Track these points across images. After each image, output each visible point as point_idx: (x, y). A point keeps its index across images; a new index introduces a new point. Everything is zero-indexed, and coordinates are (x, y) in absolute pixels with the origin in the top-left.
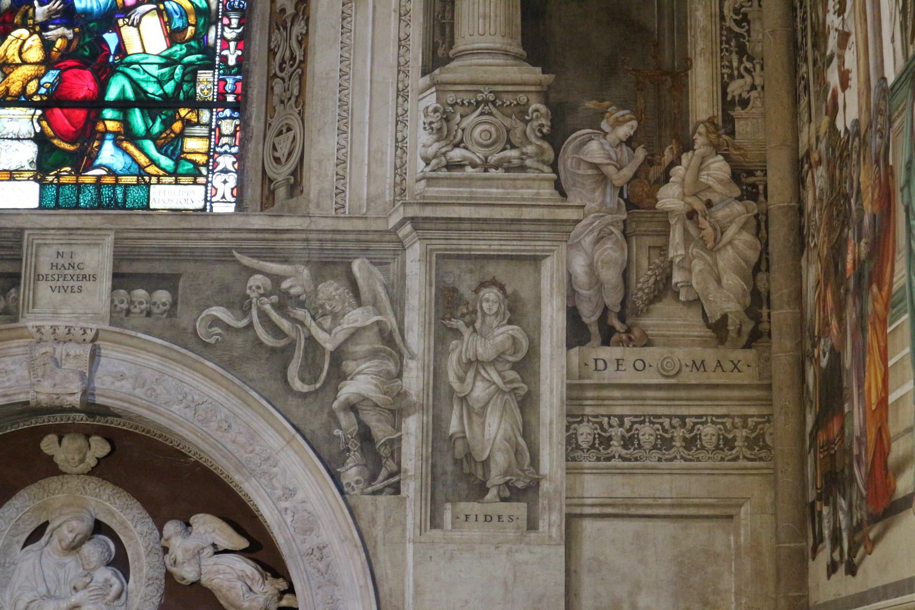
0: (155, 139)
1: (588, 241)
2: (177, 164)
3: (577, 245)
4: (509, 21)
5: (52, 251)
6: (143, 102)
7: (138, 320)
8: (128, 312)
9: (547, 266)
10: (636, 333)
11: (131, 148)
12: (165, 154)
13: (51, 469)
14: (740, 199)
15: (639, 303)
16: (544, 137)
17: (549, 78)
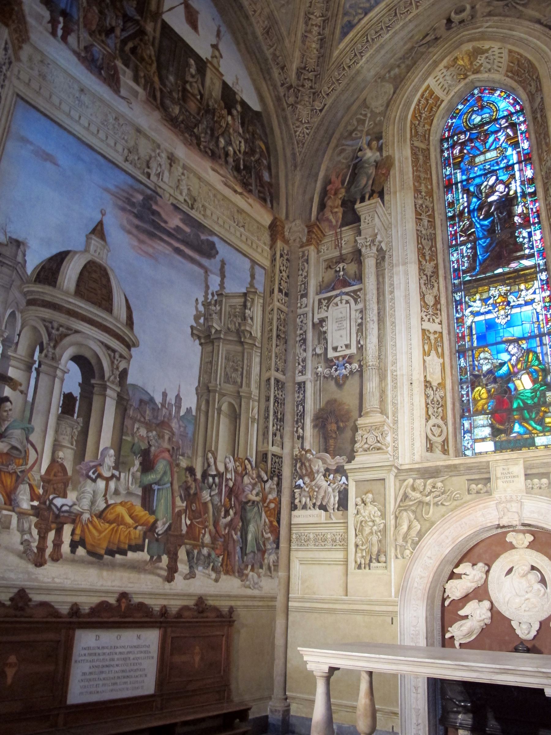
0: (534, 420)
2: (543, 428)
5: (501, 468)
6: (527, 407)
7: (536, 490)
8: (532, 488)
11: (525, 425)
12: (538, 425)
13: (512, 547)
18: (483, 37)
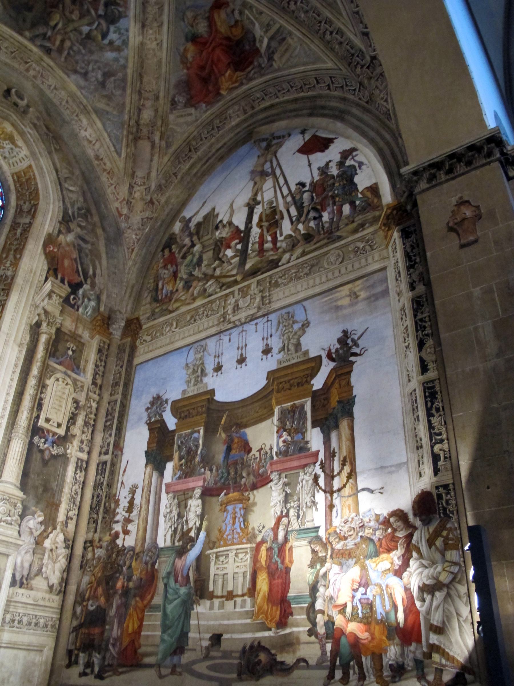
1: (23, 552)
3: (19, 553)
4: (18, 475)
9: (10, 558)
10: (29, 585)
14: (64, 548)
15: (32, 576)
16: (19, 516)
17: (25, 497)
18: (22, 134)
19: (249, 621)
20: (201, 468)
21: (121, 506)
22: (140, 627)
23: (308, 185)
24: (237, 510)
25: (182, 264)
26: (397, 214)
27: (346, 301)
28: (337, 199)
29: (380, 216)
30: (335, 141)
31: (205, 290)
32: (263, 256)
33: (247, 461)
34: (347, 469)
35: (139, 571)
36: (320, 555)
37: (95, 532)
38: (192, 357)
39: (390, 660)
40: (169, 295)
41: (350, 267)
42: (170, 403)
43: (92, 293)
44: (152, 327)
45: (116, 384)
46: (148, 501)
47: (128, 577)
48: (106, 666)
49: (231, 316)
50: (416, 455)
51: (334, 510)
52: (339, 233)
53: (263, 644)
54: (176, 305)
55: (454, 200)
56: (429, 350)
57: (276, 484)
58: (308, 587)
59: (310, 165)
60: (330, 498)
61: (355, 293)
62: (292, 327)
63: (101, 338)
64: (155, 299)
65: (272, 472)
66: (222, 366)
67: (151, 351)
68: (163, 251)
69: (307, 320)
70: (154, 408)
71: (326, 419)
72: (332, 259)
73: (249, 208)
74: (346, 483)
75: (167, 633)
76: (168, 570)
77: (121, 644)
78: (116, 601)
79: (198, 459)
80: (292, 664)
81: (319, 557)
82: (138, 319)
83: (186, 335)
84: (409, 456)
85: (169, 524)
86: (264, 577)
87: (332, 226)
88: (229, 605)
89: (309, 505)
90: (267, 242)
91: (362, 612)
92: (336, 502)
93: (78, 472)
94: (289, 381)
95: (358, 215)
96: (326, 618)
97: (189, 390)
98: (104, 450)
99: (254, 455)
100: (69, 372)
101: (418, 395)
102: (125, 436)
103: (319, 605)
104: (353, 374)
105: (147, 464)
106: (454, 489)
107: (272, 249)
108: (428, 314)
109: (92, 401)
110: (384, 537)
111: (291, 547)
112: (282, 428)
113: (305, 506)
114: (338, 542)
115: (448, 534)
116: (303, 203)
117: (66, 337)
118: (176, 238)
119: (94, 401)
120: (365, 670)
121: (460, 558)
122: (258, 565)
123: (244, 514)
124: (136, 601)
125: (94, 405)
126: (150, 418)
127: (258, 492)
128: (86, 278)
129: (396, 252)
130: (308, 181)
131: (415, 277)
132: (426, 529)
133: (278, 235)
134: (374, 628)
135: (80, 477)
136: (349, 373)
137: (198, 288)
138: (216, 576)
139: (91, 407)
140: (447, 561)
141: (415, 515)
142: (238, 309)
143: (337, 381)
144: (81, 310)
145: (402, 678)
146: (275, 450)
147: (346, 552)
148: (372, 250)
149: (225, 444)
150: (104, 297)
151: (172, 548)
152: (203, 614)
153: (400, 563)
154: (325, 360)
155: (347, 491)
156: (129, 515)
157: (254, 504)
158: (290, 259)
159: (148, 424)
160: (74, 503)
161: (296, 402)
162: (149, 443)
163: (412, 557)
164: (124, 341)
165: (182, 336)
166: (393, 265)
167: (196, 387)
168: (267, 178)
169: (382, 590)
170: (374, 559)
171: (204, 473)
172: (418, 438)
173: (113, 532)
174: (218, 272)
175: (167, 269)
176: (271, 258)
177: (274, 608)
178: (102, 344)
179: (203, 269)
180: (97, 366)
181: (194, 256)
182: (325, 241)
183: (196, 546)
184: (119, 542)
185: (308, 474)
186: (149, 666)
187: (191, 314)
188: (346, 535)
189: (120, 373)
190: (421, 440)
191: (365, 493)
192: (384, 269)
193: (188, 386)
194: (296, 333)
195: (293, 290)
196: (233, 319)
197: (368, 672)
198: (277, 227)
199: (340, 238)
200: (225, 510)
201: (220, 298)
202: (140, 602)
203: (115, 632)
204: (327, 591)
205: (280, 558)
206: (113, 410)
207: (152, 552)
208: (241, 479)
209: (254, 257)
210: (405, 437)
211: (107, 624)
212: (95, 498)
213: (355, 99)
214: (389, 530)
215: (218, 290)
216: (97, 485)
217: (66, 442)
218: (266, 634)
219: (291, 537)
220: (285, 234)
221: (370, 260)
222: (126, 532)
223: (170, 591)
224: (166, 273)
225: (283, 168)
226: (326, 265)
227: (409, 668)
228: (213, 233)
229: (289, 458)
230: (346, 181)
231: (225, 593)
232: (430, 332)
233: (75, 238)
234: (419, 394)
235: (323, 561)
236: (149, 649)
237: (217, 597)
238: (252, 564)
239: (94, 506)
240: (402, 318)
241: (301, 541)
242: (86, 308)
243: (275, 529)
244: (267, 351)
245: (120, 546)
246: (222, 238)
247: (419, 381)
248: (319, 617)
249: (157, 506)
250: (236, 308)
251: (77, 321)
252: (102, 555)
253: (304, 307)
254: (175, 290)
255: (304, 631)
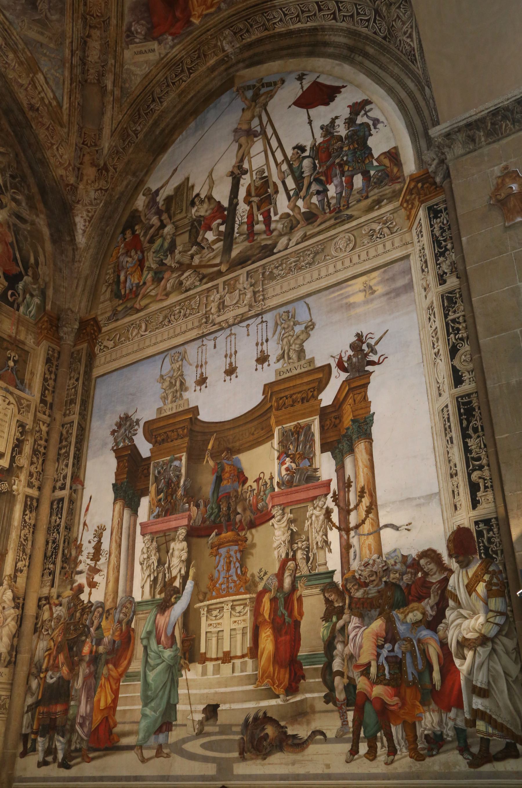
14: (13, 608)
19: (251, 687)
20: (184, 504)
21: (85, 553)
22: (115, 701)
23: (308, 148)
24: (232, 553)
25: (150, 249)
26: (422, 187)
27: (359, 298)
28: (346, 168)
29: (401, 190)
30: (342, 90)
31: (181, 283)
32: (253, 241)
33: (242, 494)
34: (366, 501)
35: (111, 632)
36: (336, 605)
37: (52, 586)
38: (167, 367)
39: (425, 729)
40: (134, 289)
41: (364, 256)
42: (142, 424)
43: (35, 287)
44: (115, 329)
45: (72, 401)
46: (120, 546)
47: (97, 640)
48: (72, 751)
49: (215, 316)
50: (450, 484)
51: (352, 551)
52: (349, 212)
53: (269, 715)
54: (143, 303)
55: (497, 170)
56: (463, 357)
57: (279, 521)
58: (322, 644)
59: (310, 122)
60: (345, 537)
61: (371, 288)
62: (293, 329)
63: (49, 343)
64: (117, 295)
65: (273, 507)
66: (207, 378)
67: (114, 360)
68: (123, 232)
69: (311, 321)
70: (122, 430)
71: (339, 442)
72: (342, 244)
73: (233, 179)
74: (365, 519)
75: (149, 706)
76: (148, 630)
77: (91, 723)
78: (83, 670)
79: (180, 492)
80: (306, 738)
81: (335, 607)
82: (95, 320)
83: (159, 339)
84: (441, 486)
85: (147, 573)
86: (268, 633)
87: (340, 204)
88: (226, 668)
89: (320, 545)
90: (258, 223)
91: (389, 673)
92: (354, 541)
93: (28, 512)
94: (291, 396)
95: (372, 190)
96: (346, 681)
97: (165, 407)
98: (59, 484)
99: (251, 486)
100: (11, 389)
101: (451, 412)
102: (86, 465)
103: (337, 665)
104: (370, 386)
105: (116, 500)
106: (498, 525)
107: (265, 232)
108: (463, 313)
109: (41, 423)
110: (413, 582)
111: (301, 596)
112: (284, 453)
113: (315, 547)
114: (357, 590)
115: (491, 579)
116: (303, 173)
117: (5, 344)
118: (140, 216)
119: (44, 423)
120: (396, 742)
121: (507, 606)
122: (260, 619)
123: (242, 557)
124: (109, 670)
125: (44, 428)
126: (117, 444)
127: (257, 531)
128: (26, 269)
129: (422, 236)
130: (308, 144)
131: (445, 267)
132: (464, 572)
133: (272, 214)
134: (405, 692)
135: (30, 518)
136: (365, 386)
137: (172, 281)
138: (208, 635)
139: (40, 431)
140: (491, 611)
141: (450, 556)
142: (224, 307)
143: (351, 395)
144: (22, 309)
145: (441, 750)
146: (276, 479)
147: (368, 601)
148: (392, 233)
149: (213, 474)
150: (50, 292)
151: (152, 602)
152: (194, 680)
153: (434, 613)
154: (335, 371)
155: (367, 527)
156: (96, 564)
157: (253, 546)
158: (288, 244)
159: (115, 451)
160: (24, 551)
161: (299, 422)
162: (117, 474)
163: (448, 606)
164: (78, 347)
165: (153, 341)
166: (418, 252)
167: (175, 404)
168: (255, 139)
169: (413, 645)
170: (401, 610)
171: (189, 510)
172: (452, 464)
173: (76, 584)
174: (196, 261)
175: (131, 257)
176: (263, 243)
177: (282, 671)
178: (50, 352)
179: (177, 256)
180: (45, 380)
181: (164, 239)
182: (332, 222)
183: (182, 598)
184: (84, 597)
185: (318, 509)
186: (129, 748)
187: (164, 313)
188: (367, 581)
189: (75, 387)
190: (456, 466)
191: (389, 530)
192: (407, 257)
193: (165, 404)
194: (298, 337)
195: (293, 284)
196: (218, 320)
197: (399, 744)
198: (271, 204)
199: (350, 218)
200: (217, 554)
201: (200, 293)
202: (114, 669)
203: (83, 709)
204: (346, 649)
205: (287, 610)
206: (69, 434)
207: (127, 608)
208: (235, 516)
209: (243, 241)
210: (436, 462)
211: (72, 700)
212: (50, 544)
213: (369, 33)
214: (420, 575)
215: (198, 283)
216: (53, 528)
217: (12, 476)
218: (273, 702)
219: (300, 585)
220: (280, 212)
221: (388, 245)
222: (92, 585)
223: (152, 654)
224: (128, 262)
225: (276, 126)
226: (333, 253)
227: (449, 739)
228: (187, 211)
229: (293, 489)
230: (357, 144)
231: (221, 655)
232: (465, 335)
233: (10, 216)
234: (452, 410)
235: (340, 613)
236: (127, 728)
237: (211, 660)
238: (253, 618)
239: (49, 554)
240: (430, 319)
241: (312, 588)
242: (28, 306)
243: (280, 576)
244: (262, 359)
245: (85, 602)
246: (200, 216)
247: (452, 396)
248: (337, 679)
249: (130, 551)
250: (221, 306)
251: (18, 324)
252: (62, 614)
253: (308, 305)
254: (141, 283)
255: (319, 697)
